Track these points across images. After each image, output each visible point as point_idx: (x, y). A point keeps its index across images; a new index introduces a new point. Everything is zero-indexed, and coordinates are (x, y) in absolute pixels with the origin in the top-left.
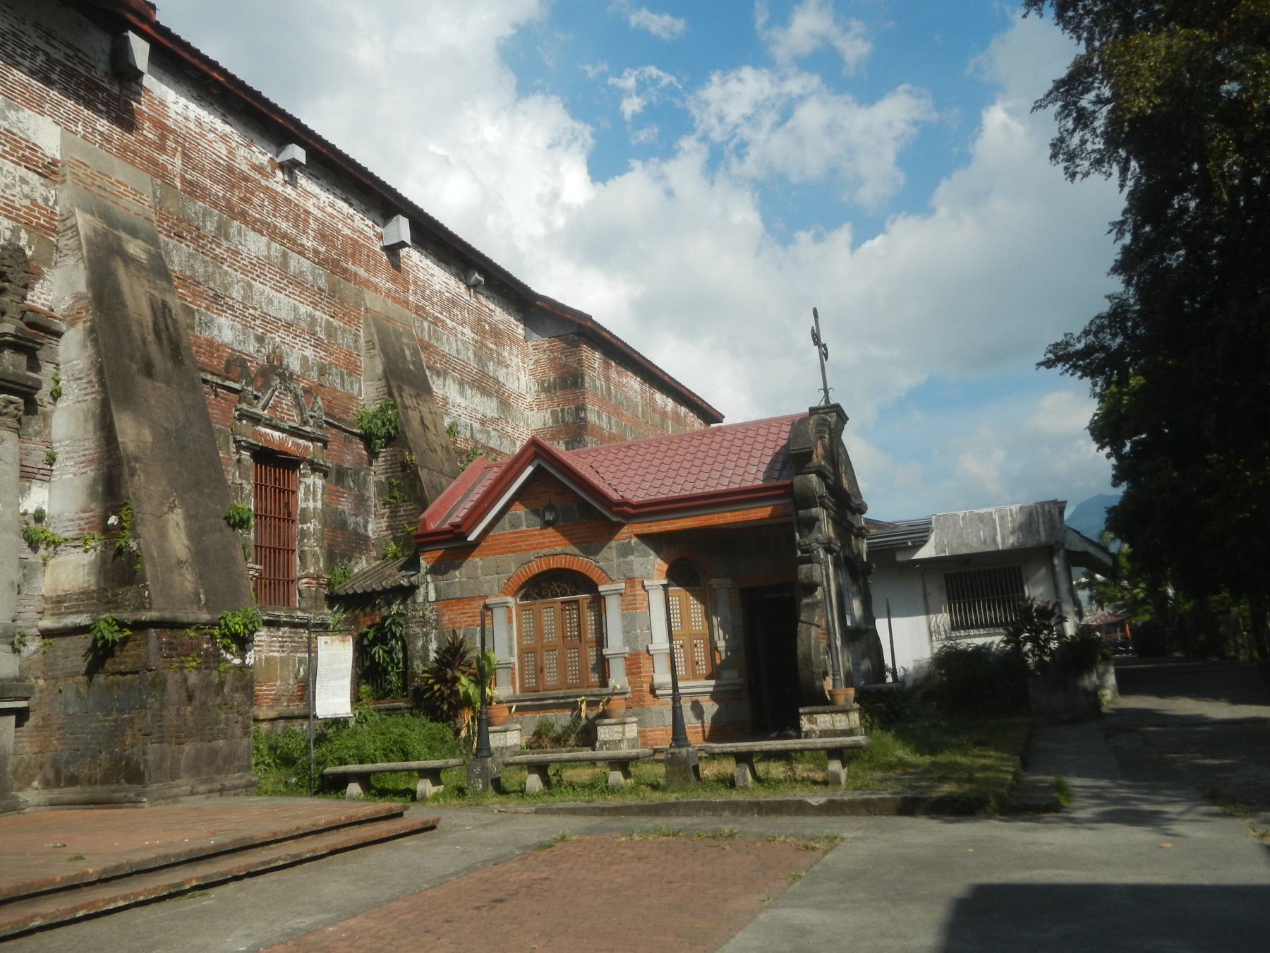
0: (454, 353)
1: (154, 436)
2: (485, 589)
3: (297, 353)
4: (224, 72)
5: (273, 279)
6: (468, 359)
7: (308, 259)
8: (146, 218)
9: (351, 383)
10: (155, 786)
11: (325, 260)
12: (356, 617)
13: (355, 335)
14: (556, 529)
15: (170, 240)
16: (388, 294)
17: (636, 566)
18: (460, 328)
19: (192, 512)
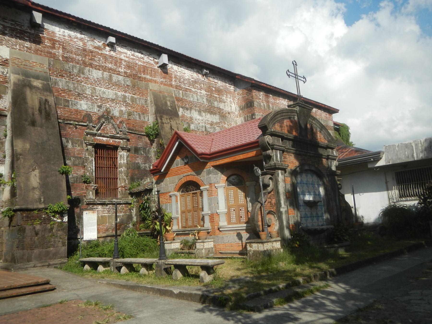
0: (196, 100)
1: (30, 146)
2: (170, 189)
3: (117, 109)
4: (74, 17)
5: (105, 85)
6: (203, 102)
8: (45, 72)
10: (19, 265)
11: (131, 75)
12: (138, 200)
13: (146, 99)
14: (189, 166)
15: (57, 78)
16: (162, 83)
17: (212, 178)
18: (199, 91)
19: (43, 170)
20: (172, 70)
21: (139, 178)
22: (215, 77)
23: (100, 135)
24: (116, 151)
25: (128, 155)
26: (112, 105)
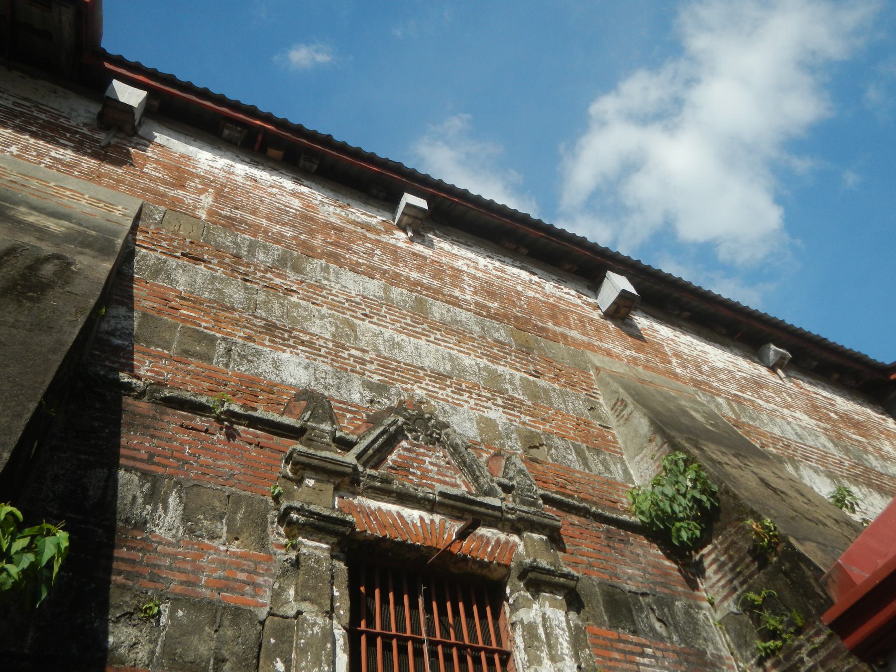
0: (793, 437)
6: (825, 446)
7: (470, 310)
9: (604, 463)
16: (634, 361)
18: (786, 411)
20: (655, 334)
22: (813, 381)
23: (384, 492)
24: (496, 615)
25: (576, 626)
26: (441, 392)
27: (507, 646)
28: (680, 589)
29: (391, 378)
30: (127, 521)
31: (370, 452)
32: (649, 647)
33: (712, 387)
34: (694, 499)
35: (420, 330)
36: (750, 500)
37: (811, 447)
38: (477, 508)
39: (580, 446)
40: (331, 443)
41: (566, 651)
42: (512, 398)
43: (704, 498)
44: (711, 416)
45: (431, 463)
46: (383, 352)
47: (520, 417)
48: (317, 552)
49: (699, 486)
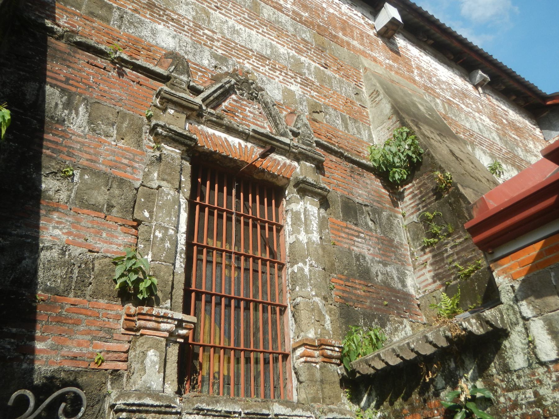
6: (494, 139)
7: (288, 16)
9: (358, 129)
16: (390, 67)
18: (477, 114)
21: (374, 316)
22: (499, 99)
23: (218, 124)
24: (277, 206)
26: (262, 68)
27: (281, 222)
28: (387, 205)
29: (230, 54)
30: (52, 118)
31: (212, 98)
32: (363, 233)
33: (435, 92)
34: (408, 156)
35: (253, 24)
36: (441, 161)
37: (485, 138)
38: (275, 143)
39: (345, 116)
40: (186, 89)
41: (315, 229)
42: (307, 79)
43: (414, 156)
44: (430, 109)
45: (250, 112)
46: (227, 35)
47: (310, 92)
48: (173, 154)
49: (412, 149)
